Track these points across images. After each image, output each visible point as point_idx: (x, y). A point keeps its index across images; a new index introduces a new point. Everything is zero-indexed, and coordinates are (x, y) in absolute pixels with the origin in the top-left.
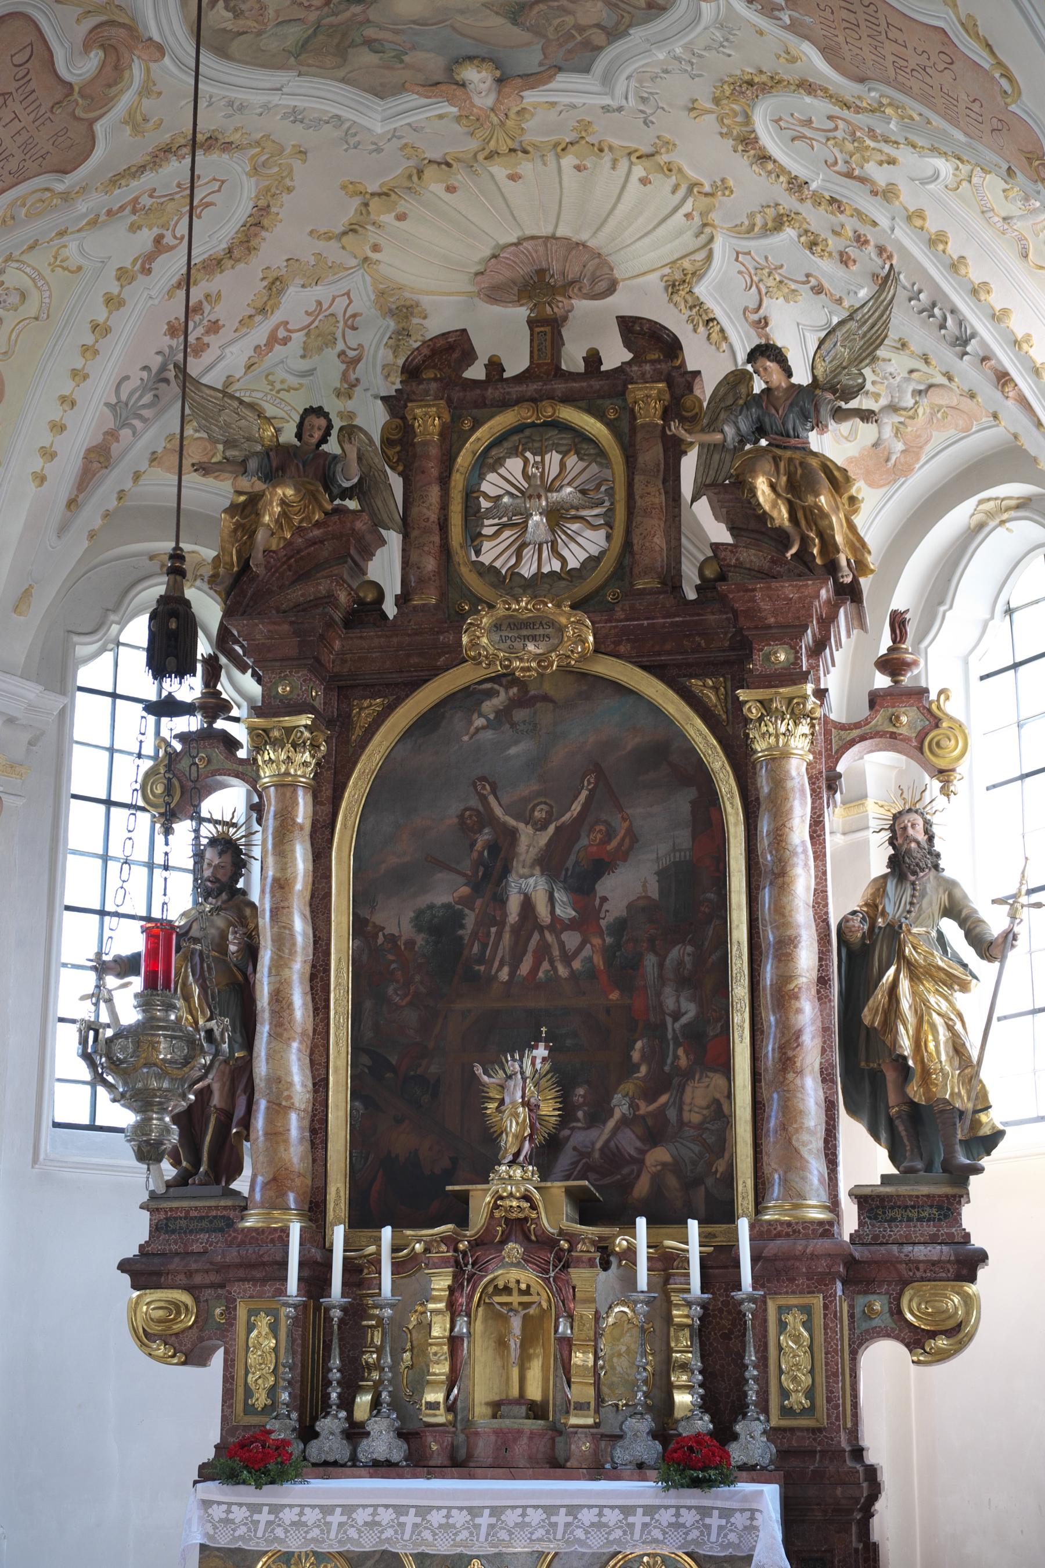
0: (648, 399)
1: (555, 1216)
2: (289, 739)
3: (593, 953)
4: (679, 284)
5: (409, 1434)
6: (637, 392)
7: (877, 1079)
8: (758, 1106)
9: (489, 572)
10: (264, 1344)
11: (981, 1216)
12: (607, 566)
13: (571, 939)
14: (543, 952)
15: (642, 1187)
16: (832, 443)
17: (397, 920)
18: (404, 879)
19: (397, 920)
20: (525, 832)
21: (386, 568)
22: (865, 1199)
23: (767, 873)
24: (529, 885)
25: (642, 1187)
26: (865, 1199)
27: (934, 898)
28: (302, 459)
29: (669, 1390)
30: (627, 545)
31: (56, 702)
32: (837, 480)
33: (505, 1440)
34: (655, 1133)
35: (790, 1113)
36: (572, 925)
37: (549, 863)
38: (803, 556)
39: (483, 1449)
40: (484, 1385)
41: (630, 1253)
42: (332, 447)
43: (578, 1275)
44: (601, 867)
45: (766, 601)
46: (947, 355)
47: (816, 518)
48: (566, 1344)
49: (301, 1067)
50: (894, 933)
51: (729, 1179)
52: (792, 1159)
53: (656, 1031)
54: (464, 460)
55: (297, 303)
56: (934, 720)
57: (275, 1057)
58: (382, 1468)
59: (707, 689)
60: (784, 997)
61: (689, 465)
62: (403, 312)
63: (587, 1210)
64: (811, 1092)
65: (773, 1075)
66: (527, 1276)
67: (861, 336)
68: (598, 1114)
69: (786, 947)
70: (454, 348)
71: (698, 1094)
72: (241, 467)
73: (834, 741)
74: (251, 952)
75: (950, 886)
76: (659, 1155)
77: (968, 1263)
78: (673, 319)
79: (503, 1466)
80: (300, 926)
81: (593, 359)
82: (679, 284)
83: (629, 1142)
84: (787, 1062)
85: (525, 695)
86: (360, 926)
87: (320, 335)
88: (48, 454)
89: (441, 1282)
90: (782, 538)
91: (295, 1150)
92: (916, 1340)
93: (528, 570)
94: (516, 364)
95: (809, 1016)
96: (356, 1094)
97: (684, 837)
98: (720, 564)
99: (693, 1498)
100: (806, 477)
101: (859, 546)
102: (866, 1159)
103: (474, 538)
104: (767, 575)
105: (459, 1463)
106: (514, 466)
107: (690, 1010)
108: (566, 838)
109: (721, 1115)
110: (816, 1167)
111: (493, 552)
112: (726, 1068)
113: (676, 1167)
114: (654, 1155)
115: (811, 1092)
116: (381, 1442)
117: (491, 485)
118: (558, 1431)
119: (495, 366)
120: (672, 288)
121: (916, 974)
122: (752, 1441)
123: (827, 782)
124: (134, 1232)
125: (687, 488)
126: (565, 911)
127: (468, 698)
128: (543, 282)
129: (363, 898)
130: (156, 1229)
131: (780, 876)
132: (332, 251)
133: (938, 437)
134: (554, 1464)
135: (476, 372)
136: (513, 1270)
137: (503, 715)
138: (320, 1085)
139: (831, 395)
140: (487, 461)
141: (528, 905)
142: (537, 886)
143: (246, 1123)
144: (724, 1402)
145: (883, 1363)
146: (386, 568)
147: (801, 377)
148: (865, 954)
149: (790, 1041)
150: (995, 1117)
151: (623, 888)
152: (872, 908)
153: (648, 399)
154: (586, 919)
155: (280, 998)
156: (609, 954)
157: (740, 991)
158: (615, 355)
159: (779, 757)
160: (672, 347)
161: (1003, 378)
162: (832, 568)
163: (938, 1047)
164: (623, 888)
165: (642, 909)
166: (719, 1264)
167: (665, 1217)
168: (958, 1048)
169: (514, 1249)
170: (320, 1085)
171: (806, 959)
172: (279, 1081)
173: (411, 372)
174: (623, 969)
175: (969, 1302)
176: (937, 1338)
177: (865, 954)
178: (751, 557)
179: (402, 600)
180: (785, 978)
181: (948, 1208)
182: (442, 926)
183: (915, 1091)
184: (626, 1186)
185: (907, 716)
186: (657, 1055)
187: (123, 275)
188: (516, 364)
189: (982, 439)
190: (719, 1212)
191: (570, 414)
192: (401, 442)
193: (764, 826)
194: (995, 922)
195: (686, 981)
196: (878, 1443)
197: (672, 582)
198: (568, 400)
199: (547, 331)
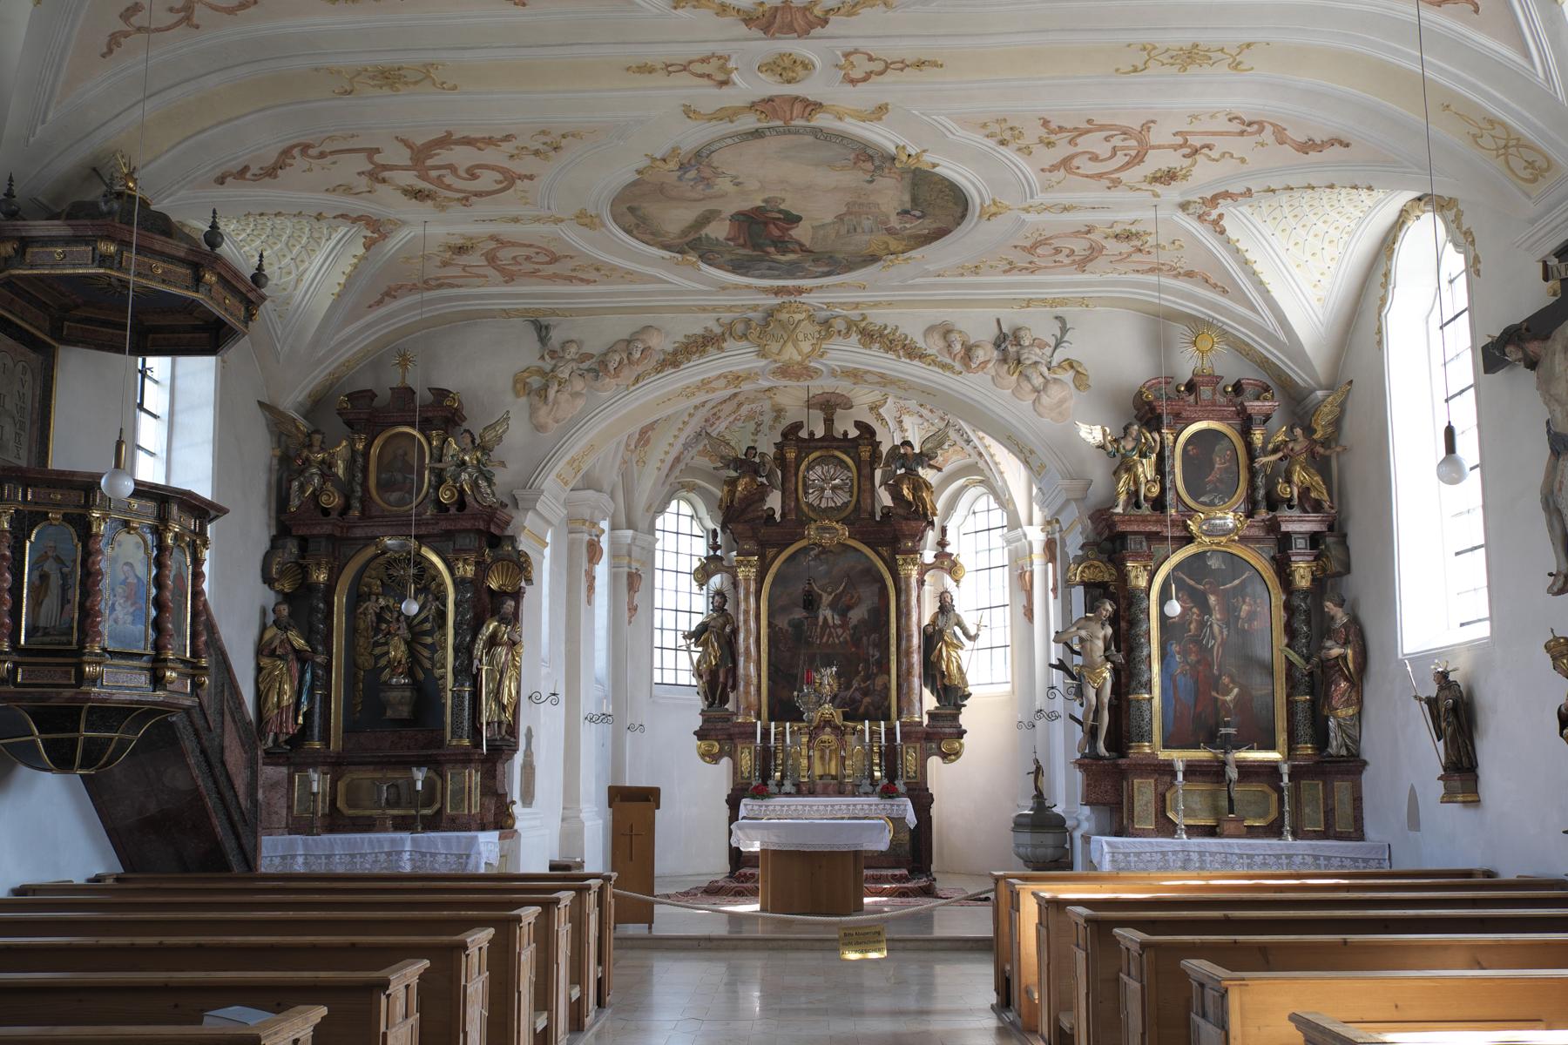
0: (865, 452)
1: (838, 721)
2: (748, 564)
3: (846, 636)
4: (874, 408)
5: (797, 785)
6: (862, 448)
7: (934, 677)
8: (899, 685)
9: (810, 505)
10: (746, 760)
11: (965, 719)
12: (851, 507)
13: (840, 631)
14: (830, 635)
15: (862, 710)
16: (926, 474)
17: (783, 623)
18: (785, 609)
19: (783, 623)
20: (825, 595)
21: (774, 501)
22: (930, 714)
23: (903, 613)
24: (825, 613)
25: (862, 710)
26: (930, 714)
27: (954, 620)
28: (747, 464)
29: (872, 771)
30: (858, 501)
31: (649, 538)
32: (928, 486)
33: (826, 787)
34: (866, 693)
35: (910, 688)
36: (840, 626)
37: (833, 606)
38: (916, 511)
39: (819, 789)
40: (818, 770)
41: (863, 731)
42: (757, 460)
43: (847, 737)
44: (849, 608)
45: (907, 527)
46: (964, 444)
47: (922, 500)
48: (844, 758)
49: (753, 670)
50: (941, 632)
51: (889, 708)
52: (910, 703)
53: (867, 661)
54: (803, 467)
55: (744, 410)
56: (955, 564)
57: (746, 668)
58: (788, 794)
59: (884, 551)
60: (908, 653)
61: (878, 473)
62: (779, 412)
63: (846, 717)
64: (916, 681)
65: (904, 677)
66: (832, 738)
67: (938, 441)
68: (848, 687)
69: (909, 637)
70: (798, 426)
71: (879, 681)
72: (727, 466)
73: (924, 569)
74: (735, 632)
75: (958, 616)
76: (867, 700)
77: (961, 733)
78: (876, 425)
79: (825, 793)
80: (752, 624)
81: (846, 434)
82: (874, 408)
83: (858, 695)
84: (909, 673)
85: (824, 550)
86: (770, 625)
87: (750, 417)
88: (662, 461)
89: (805, 739)
90: (909, 504)
91: (753, 698)
92: (945, 757)
93: (823, 505)
94: (820, 433)
95: (916, 659)
96: (769, 679)
97: (876, 599)
98: (887, 513)
99: (890, 801)
100: (919, 486)
101: (934, 508)
102: (930, 702)
103: (806, 493)
104: (907, 519)
105: (812, 793)
106: (818, 469)
107: (877, 655)
108: (838, 598)
109: (887, 688)
110: (917, 705)
111: (812, 498)
112: (888, 673)
113: (872, 704)
114: (867, 701)
115: (916, 681)
116: (788, 787)
117: (812, 476)
118: (841, 783)
119: (812, 434)
120: (871, 409)
121: (947, 645)
122: (900, 785)
123: (921, 583)
124: (697, 722)
125: (877, 483)
126: (838, 622)
127: (805, 550)
128: (829, 406)
129: (771, 615)
130: (704, 721)
131: (908, 614)
132: (760, 395)
133: (955, 458)
134: (841, 793)
135: (804, 434)
136: (827, 736)
137: (817, 556)
138: (759, 676)
139: (925, 458)
140: (809, 468)
141: (825, 619)
142: (829, 613)
143: (734, 687)
144: (891, 774)
145: (934, 762)
146: (774, 501)
147: (917, 450)
148: (932, 638)
149: (910, 666)
150: (970, 689)
151: (856, 615)
152: (934, 622)
153: (865, 452)
154: (844, 625)
155: (747, 649)
156: (852, 636)
157: (893, 649)
158: (853, 433)
159: (908, 577)
160: (873, 433)
161: (980, 454)
162: (925, 515)
163: (954, 668)
164: (856, 615)
165: (862, 622)
166: (890, 732)
167: (875, 719)
168: (959, 668)
169: (828, 730)
170: (759, 676)
171: (915, 641)
172: (747, 676)
173: (784, 435)
174: (856, 642)
175: (961, 745)
176: (949, 756)
177: (932, 638)
178: (901, 511)
179: (783, 515)
180: (909, 647)
181: (955, 717)
182: (797, 626)
183: (946, 681)
184: (857, 709)
185: (947, 563)
186: (867, 668)
187: (696, 408)
188: (820, 433)
189: (968, 461)
190: (887, 718)
191: (838, 453)
192: (780, 459)
193: (903, 598)
194: (973, 632)
195: (875, 646)
196: (933, 786)
197: (873, 514)
198: (837, 448)
199: (829, 422)
